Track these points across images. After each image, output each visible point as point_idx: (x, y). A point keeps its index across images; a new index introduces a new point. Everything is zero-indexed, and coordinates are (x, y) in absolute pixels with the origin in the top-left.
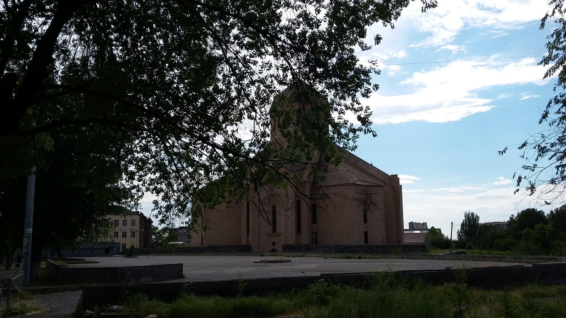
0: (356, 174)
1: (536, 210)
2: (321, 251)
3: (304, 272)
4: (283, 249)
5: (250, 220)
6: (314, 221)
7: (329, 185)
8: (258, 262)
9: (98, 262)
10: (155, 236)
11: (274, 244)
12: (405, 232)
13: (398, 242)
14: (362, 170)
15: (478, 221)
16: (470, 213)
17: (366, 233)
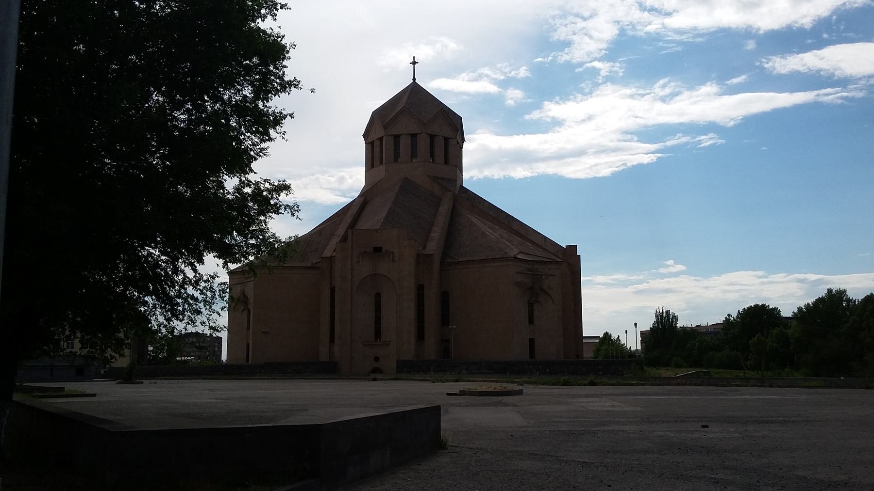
0: (515, 243)
1: (768, 306)
2: (464, 372)
3: (707, 426)
4: (397, 367)
5: (337, 317)
6: (445, 320)
7: (471, 259)
8: (455, 394)
9: (94, 395)
10: (153, 347)
11: (377, 359)
12: (584, 341)
13: (578, 356)
14: (521, 236)
15: (676, 323)
16: (664, 311)
17: (532, 341)
